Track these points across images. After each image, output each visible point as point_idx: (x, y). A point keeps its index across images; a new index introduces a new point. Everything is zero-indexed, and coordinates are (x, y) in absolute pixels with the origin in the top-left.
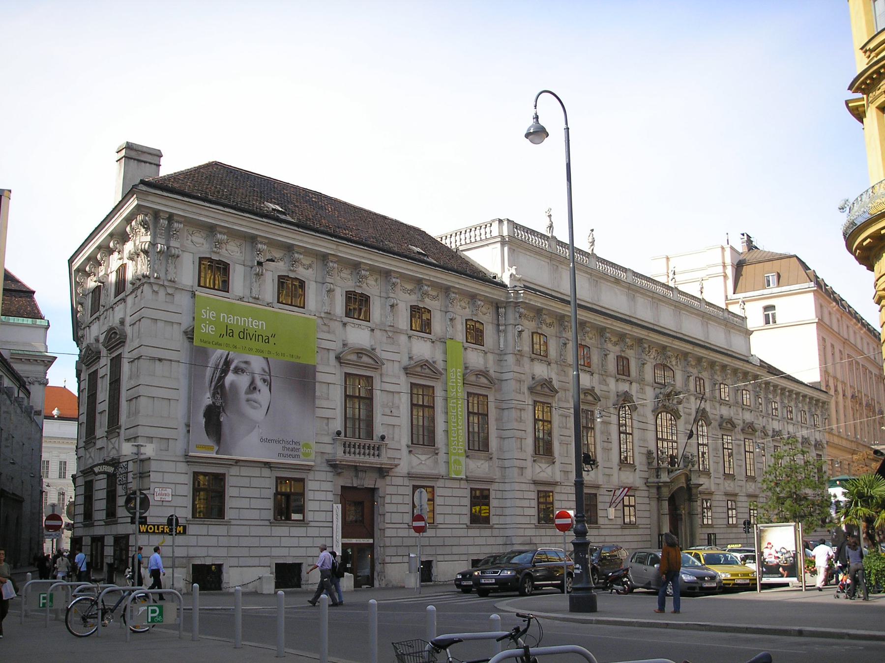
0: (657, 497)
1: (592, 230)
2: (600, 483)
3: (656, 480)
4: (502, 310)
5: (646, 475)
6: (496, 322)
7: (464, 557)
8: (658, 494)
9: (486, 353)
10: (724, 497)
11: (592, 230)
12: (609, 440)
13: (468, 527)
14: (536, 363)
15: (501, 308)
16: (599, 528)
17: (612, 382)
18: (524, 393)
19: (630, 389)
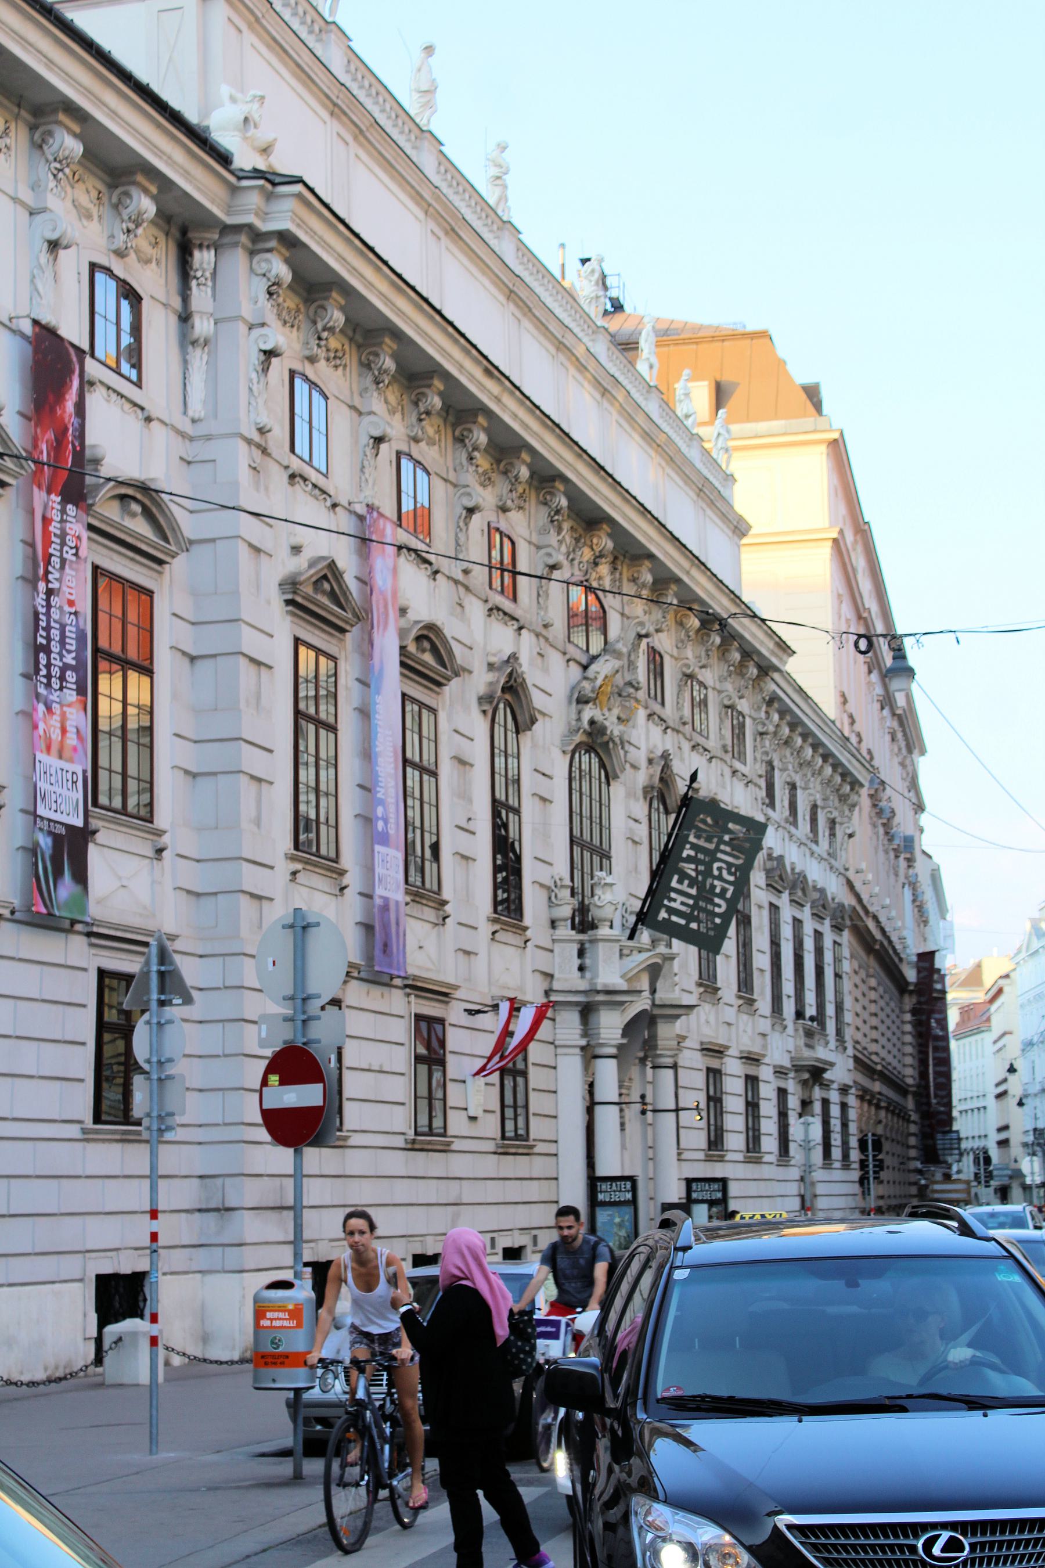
0: (583, 1042)
1: (429, 50)
2: (451, 980)
3: (583, 985)
4: (203, 259)
5: (543, 961)
6: (177, 302)
7: (71, 1266)
8: (585, 1034)
9: (148, 419)
10: (698, 1054)
11: (429, 50)
12: (471, 826)
13: (87, 1137)
14: (299, 487)
15: (201, 247)
16: (446, 1149)
17: (476, 609)
18: (269, 603)
19: (518, 643)
